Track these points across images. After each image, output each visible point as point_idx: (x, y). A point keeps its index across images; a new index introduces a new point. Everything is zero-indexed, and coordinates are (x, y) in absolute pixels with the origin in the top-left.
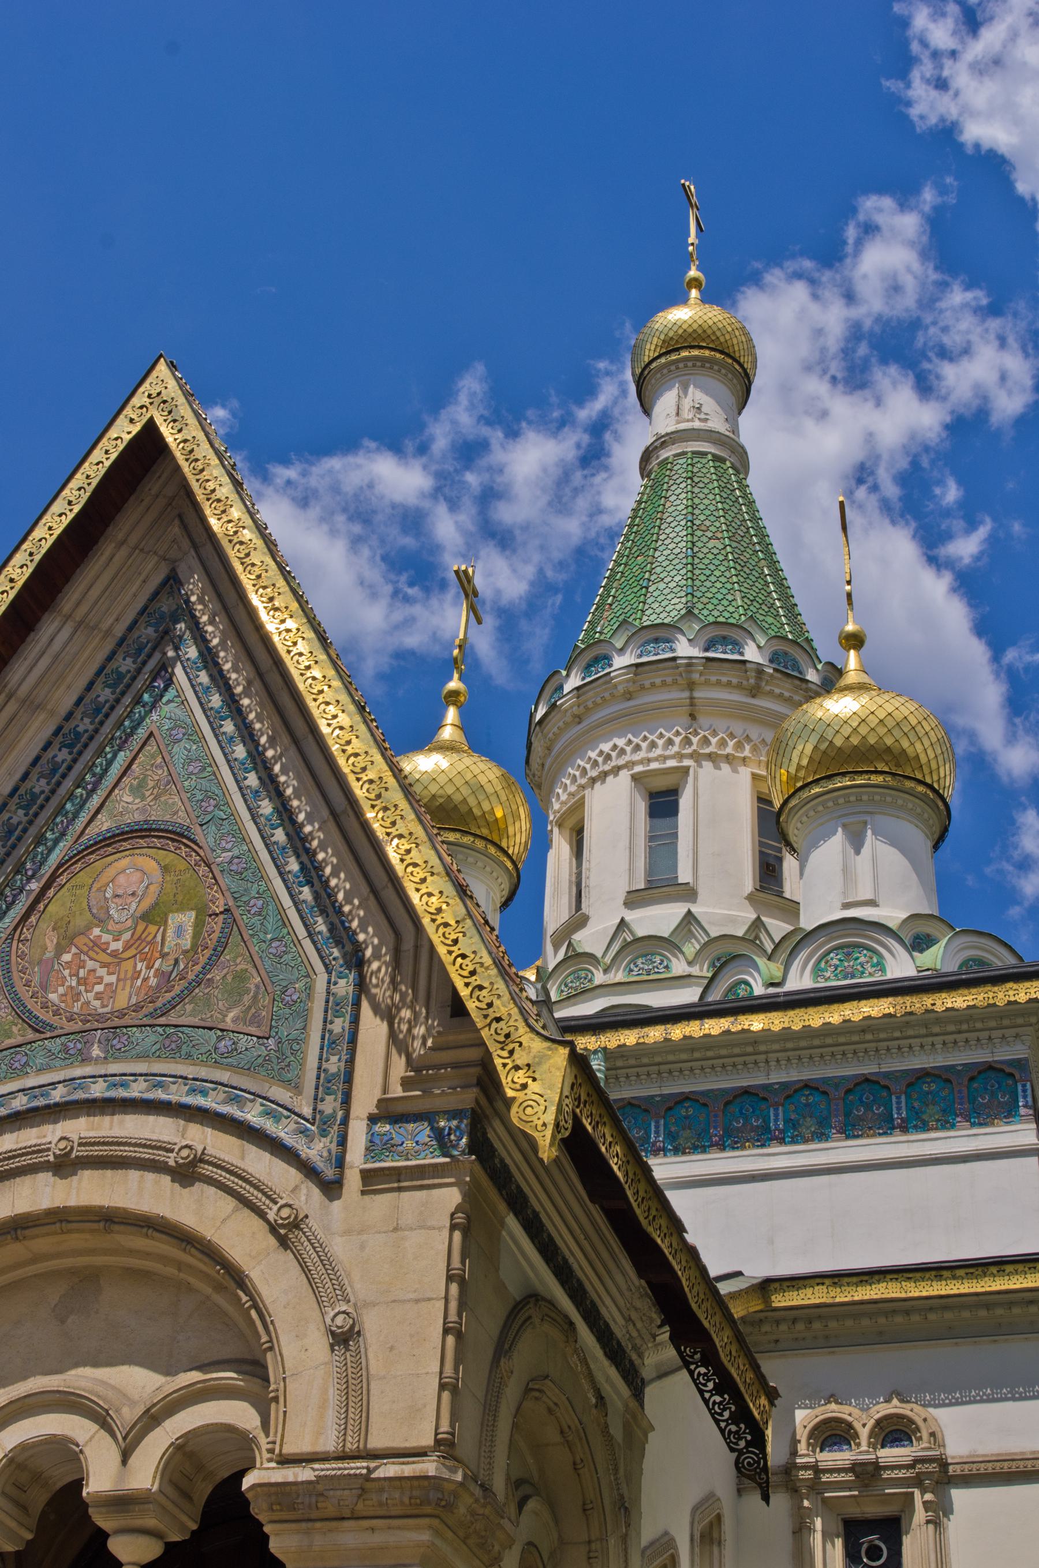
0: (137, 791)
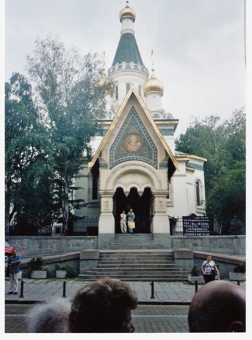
0: (133, 129)
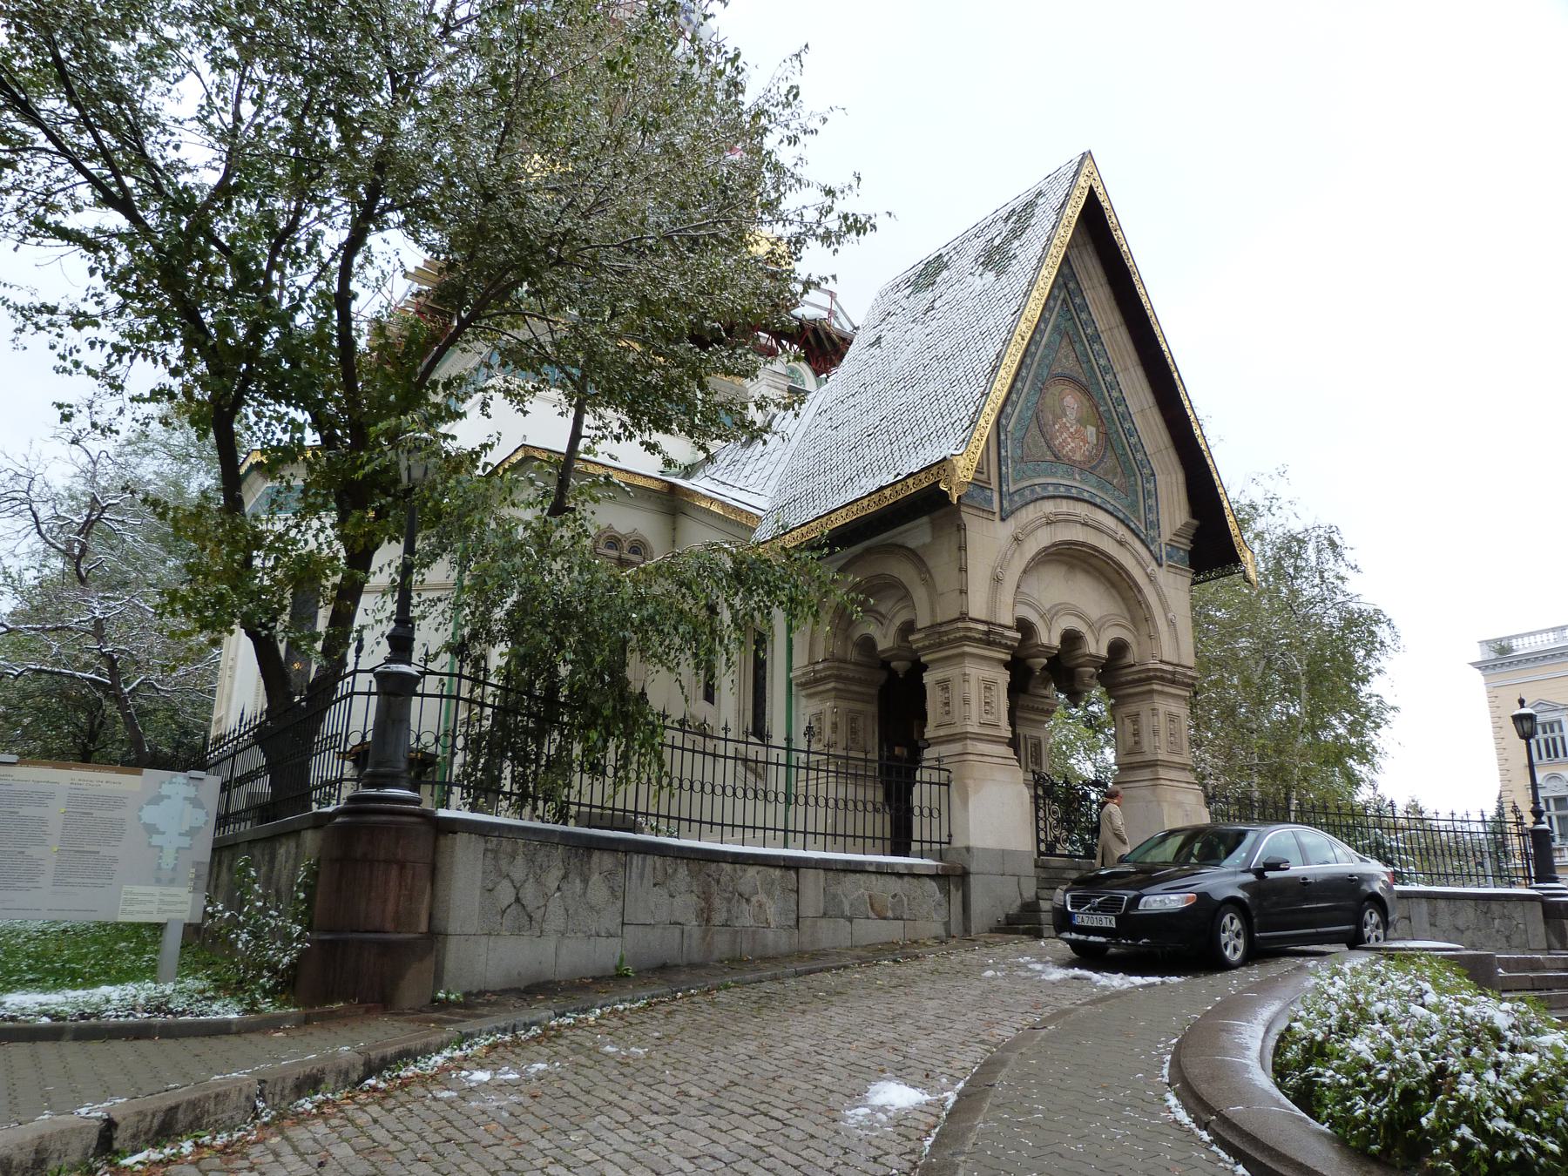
0: (1066, 357)
